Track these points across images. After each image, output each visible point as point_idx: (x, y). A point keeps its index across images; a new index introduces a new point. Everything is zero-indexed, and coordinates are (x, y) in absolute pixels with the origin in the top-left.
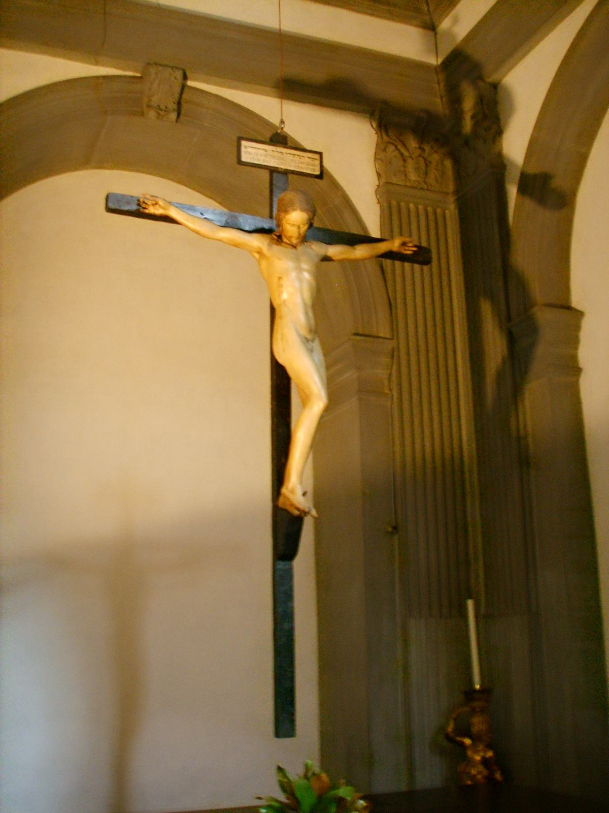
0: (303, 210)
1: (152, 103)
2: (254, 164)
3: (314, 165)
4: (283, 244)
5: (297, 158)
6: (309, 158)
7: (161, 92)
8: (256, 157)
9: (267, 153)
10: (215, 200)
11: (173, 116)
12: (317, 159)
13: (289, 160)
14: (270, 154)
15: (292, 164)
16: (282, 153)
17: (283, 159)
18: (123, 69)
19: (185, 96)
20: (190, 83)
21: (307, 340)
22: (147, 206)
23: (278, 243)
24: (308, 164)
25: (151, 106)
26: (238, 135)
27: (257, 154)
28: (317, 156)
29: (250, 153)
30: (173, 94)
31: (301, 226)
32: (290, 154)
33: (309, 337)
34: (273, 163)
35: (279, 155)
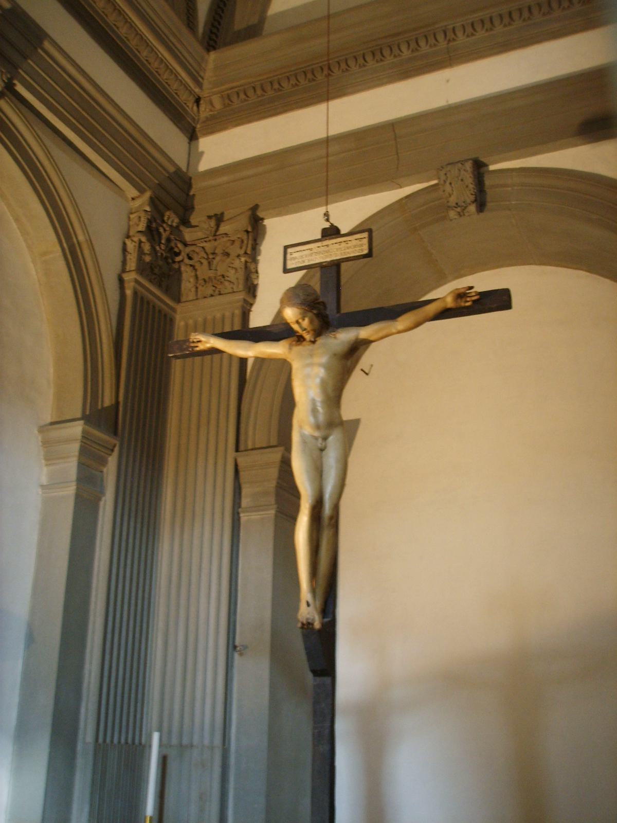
0: (293, 305)
1: (449, 204)
2: (297, 267)
3: (362, 245)
4: (304, 343)
5: (343, 245)
6: (356, 239)
7: (461, 189)
8: (300, 260)
9: (311, 252)
10: (582, 270)
11: (473, 208)
12: (365, 238)
13: (335, 250)
14: (315, 251)
15: (338, 253)
16: (327, 246)
17: (327, 252)
18: (428, 181)
19: (488, 182)
20: (492, 168)
21: (316, 438)
22: (195, 345)
23: (299, 343)
24: (355, 246)
25: (449, 207)
26: (374, 228)
27: (302, 256)
28: (366, 235)
29: (294, 258)
30: (467, 186)
31: (300, 321)
32: (336, 243)
33: (317, 434)
34: (318, 259)
35: (326, 249)
